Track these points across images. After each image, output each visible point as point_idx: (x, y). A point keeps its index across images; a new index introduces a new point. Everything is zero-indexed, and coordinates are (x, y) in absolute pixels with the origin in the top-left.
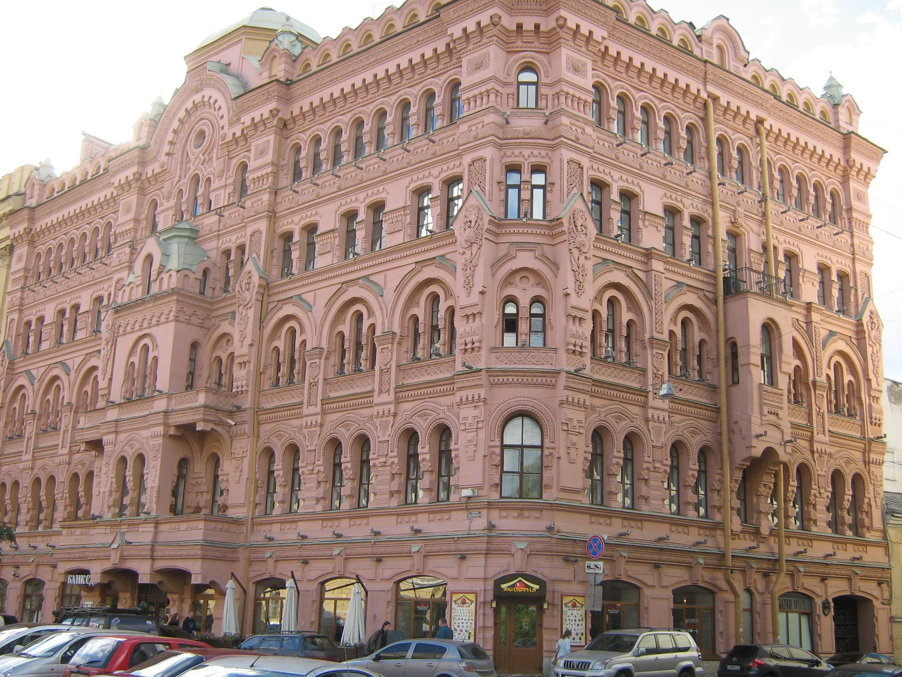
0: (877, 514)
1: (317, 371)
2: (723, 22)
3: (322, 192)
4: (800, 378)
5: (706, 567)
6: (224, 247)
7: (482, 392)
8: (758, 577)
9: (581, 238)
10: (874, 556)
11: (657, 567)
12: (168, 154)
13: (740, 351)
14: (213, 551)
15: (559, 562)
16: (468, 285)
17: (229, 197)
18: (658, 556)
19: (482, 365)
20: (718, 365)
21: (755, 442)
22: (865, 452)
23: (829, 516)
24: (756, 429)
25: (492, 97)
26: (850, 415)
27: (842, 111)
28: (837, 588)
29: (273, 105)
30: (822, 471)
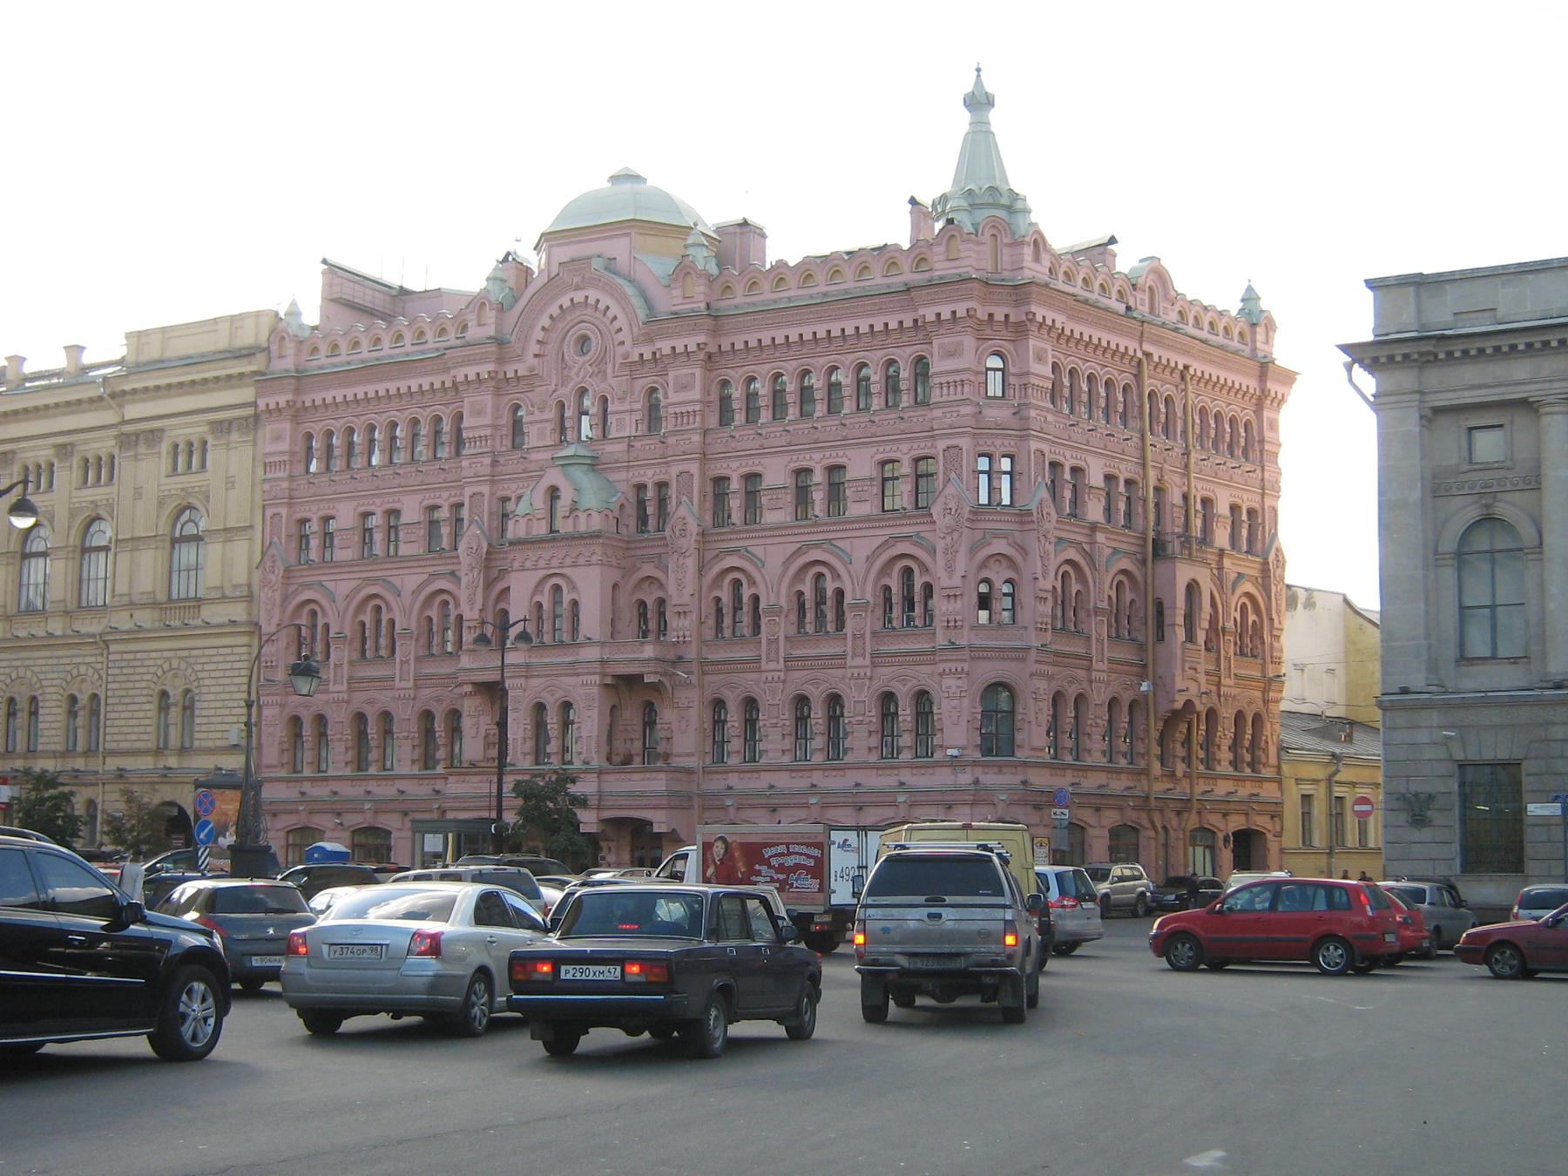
0: (1272, 750)
1: (778, 628)
2: (1155, 263)
3: (766, 443)
4: (1214, 629)
5: (1134, 808)
6: (636, 480)
7: (966, 666)
8: (1172, 815)
9: (1047, 526)
10: (1269, 791)
11: (1098, 809)
12: (536, 356)
13: (1167, 612)
14: (678, 801)
15: (1030, 809)
16: (950, 568)
18: (1099, 801)
19: (964, 642)
20: (1146, 624)
21: (1177, 697)
22: (1265, 691)
23: (1230, 756)
24: (1179, 684)
25: (967, 388)
26: (1254, 656)
27: (1260, 330)
28: (1236, 823)
29: (701, 339)
30: (1227, 714)
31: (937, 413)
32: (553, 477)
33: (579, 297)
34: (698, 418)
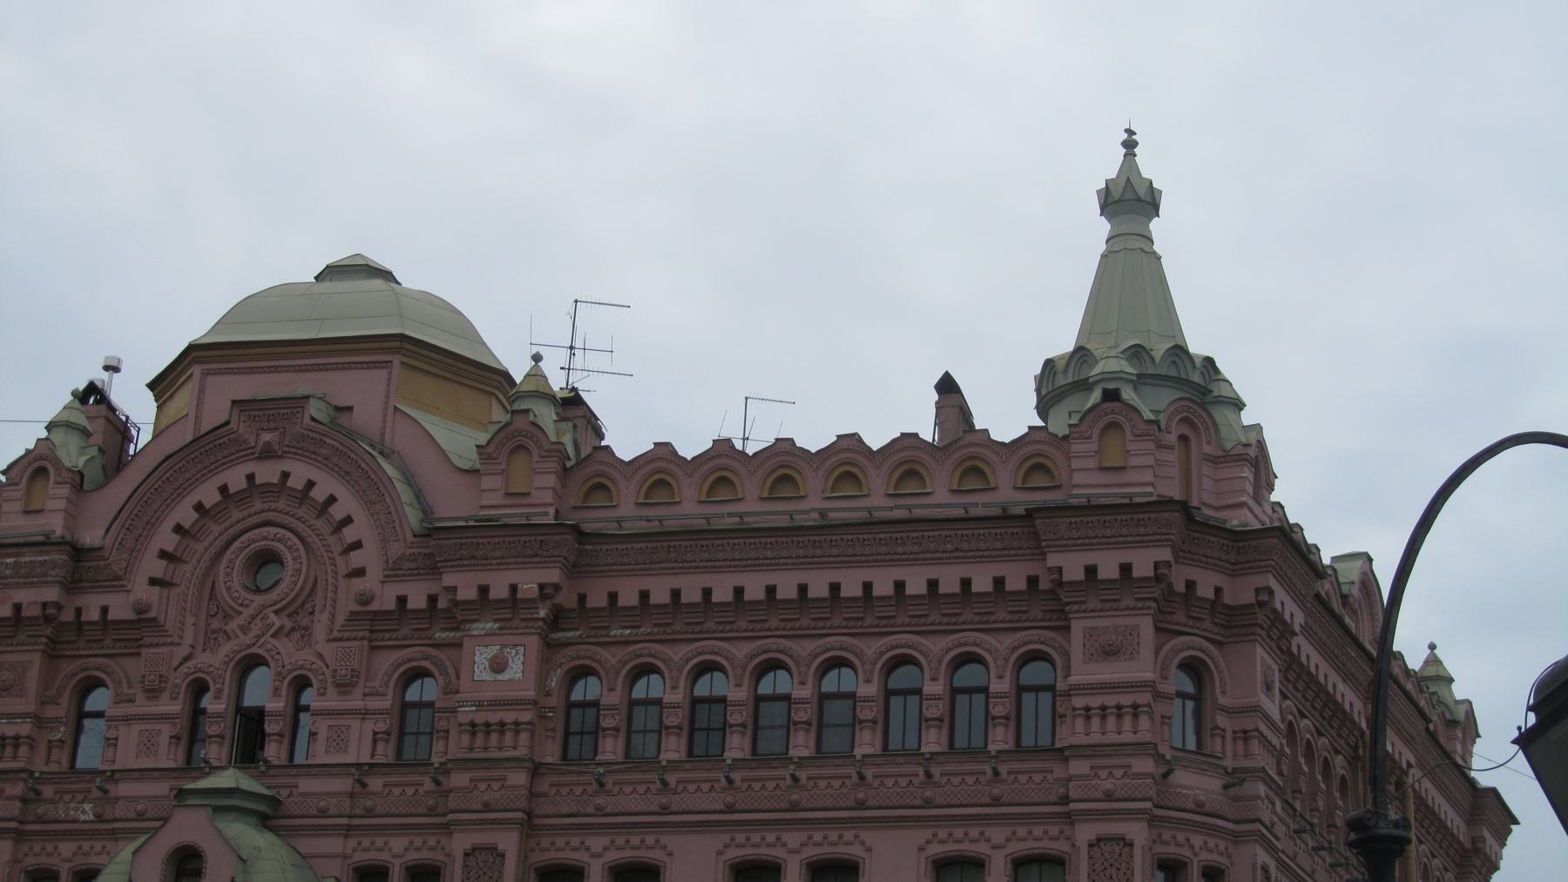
6: (360, 857)
12: (153, 582)
17: (375, 742)
25: (1144, 722)
29: (553, 575)
31: (1079, 767)
32: (188, 827)
33: (267, 473)
34: (524, 738)
